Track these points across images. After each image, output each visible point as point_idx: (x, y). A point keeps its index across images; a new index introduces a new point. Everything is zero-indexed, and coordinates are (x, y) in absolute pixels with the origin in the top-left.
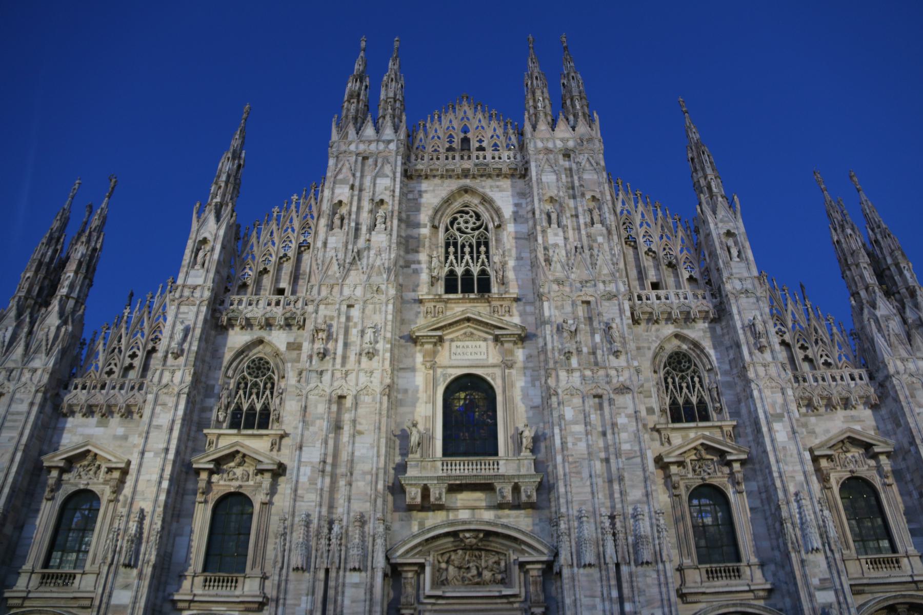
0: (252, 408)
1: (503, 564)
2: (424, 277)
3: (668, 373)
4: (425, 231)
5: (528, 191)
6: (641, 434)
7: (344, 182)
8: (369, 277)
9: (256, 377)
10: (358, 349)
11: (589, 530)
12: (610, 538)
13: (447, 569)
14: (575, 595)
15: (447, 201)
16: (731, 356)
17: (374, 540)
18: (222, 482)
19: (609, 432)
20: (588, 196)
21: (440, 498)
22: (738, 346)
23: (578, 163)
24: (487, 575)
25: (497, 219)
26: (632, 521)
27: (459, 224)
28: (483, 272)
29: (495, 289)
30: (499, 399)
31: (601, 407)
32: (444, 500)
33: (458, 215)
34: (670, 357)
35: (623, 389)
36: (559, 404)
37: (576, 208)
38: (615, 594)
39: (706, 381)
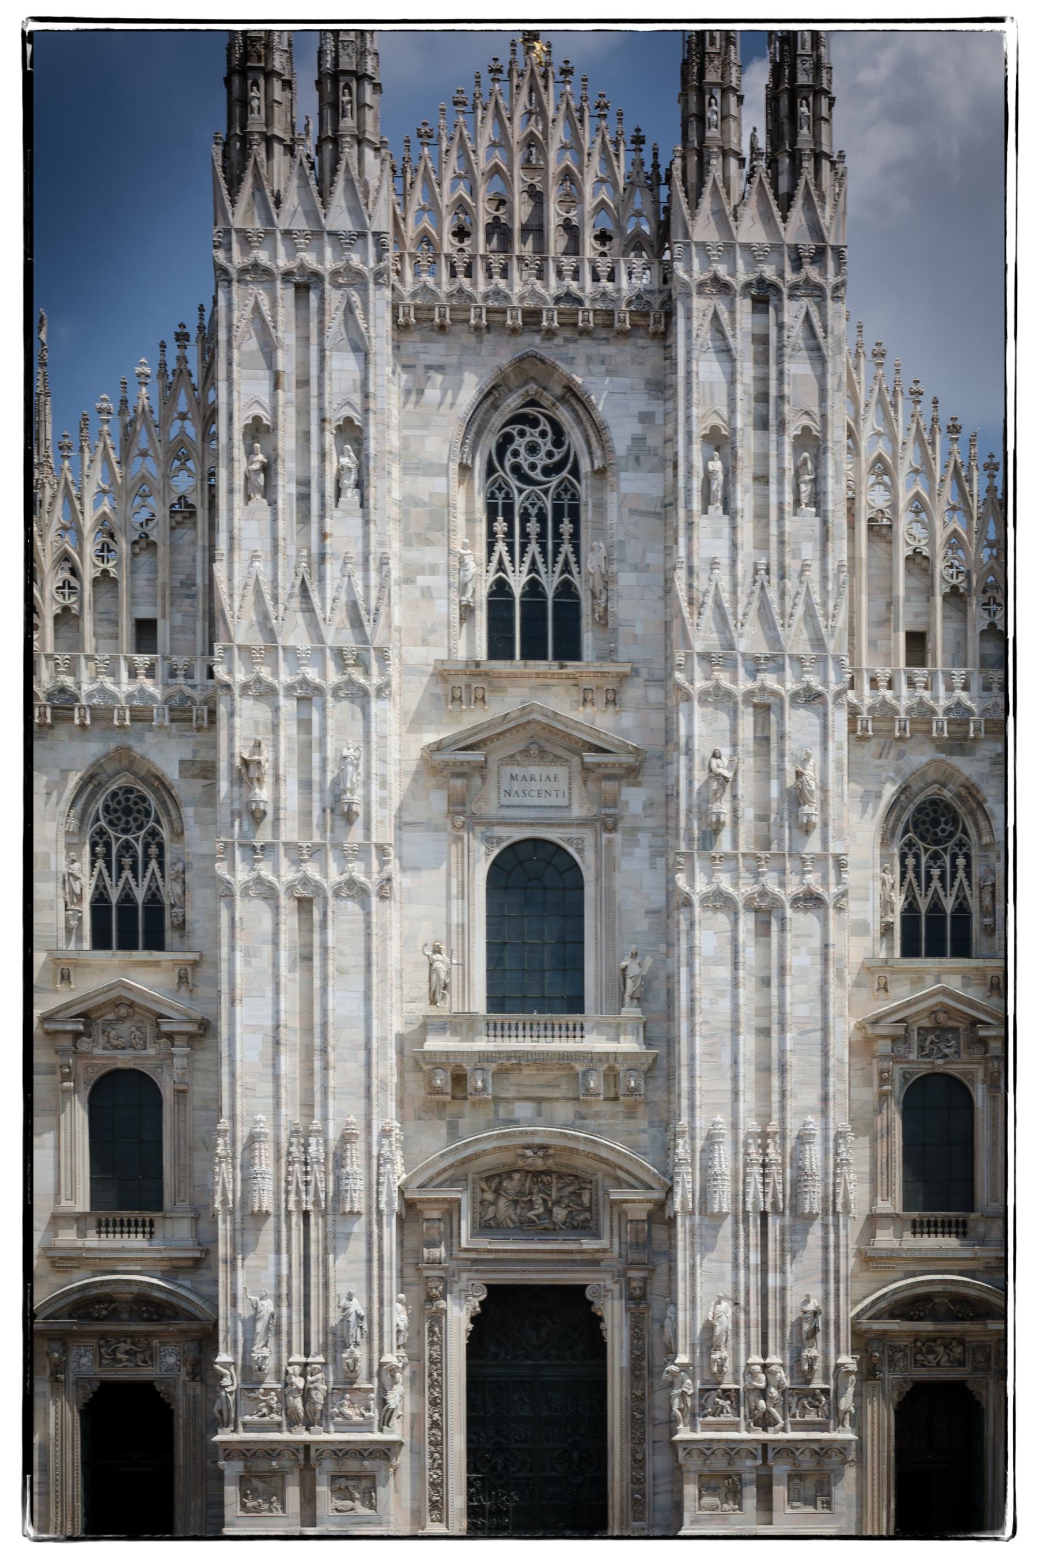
0: (127, 898)
1: (586, 1199)
2: (444, 608)
6: (832, 989)
9: (126, 831)
12: (757, 1170)
13: (494, 1203)
18: (98, 1051)
21: (484, 1088)
24: (560, 1214)
25: (598, 452)
27: (516, 454)
32: (490, 1090)
33: (514, 429)
35: (811, 900)
38: (755, 1258)
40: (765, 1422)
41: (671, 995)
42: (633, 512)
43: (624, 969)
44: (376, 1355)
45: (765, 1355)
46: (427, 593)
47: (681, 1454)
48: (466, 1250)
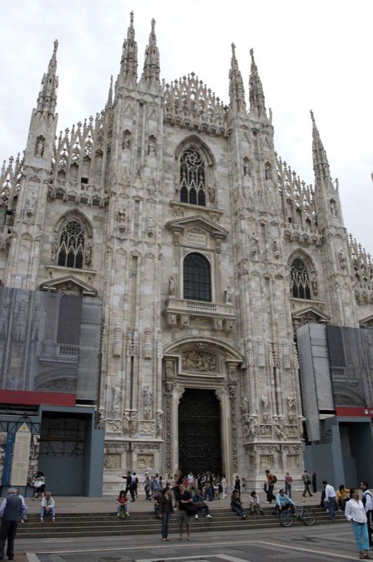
0: (71, 254)
1: (214, 362)
2: (171, 189)
3: (293, 269)
4: (172, 160)
5: (229, 148)
7: (130, 117)
8: (148, 185)
10: (144, 229)
11: (262, 350)
13: (186, 361)
14: (255, 381)
15: (183, 143)
16: (325, 267)
17: (157, 343)
19: (272, 298)
20: (266, 161)
22: (331, 263)
23: (260, 139)
25: (211, 161)
26: (281, 347)
28: (201, 192)
29: (208, 204)
30: (213, 269)
31: (267, 284)
33: (188, 153)
34: (294, 261)
35: (279, 277)
36: (249, 279)
37: (259, 167)
38: (273, 382)
39: (311, 278)
40: (279, 437)
41: (238, 301)
42: (221, 176)
43: (226, 292)
44: (155, 410)
45: (278, 413)
46: (167, 184)
47: (255, 448)
48: (180, 375)
